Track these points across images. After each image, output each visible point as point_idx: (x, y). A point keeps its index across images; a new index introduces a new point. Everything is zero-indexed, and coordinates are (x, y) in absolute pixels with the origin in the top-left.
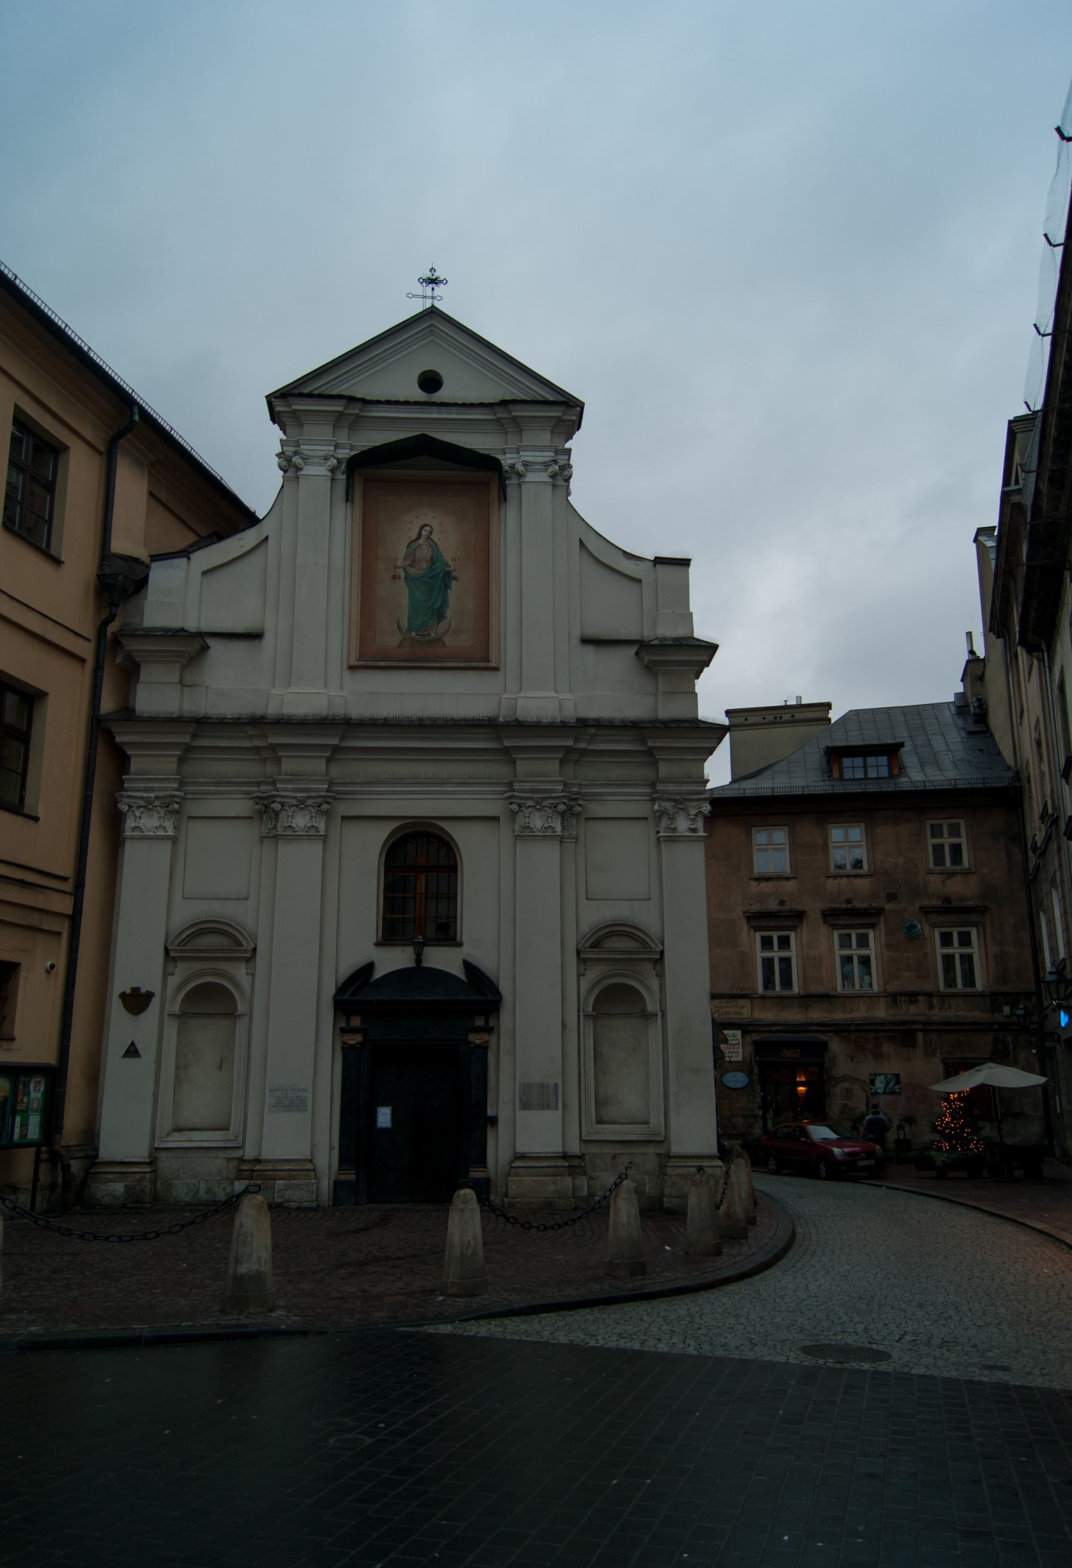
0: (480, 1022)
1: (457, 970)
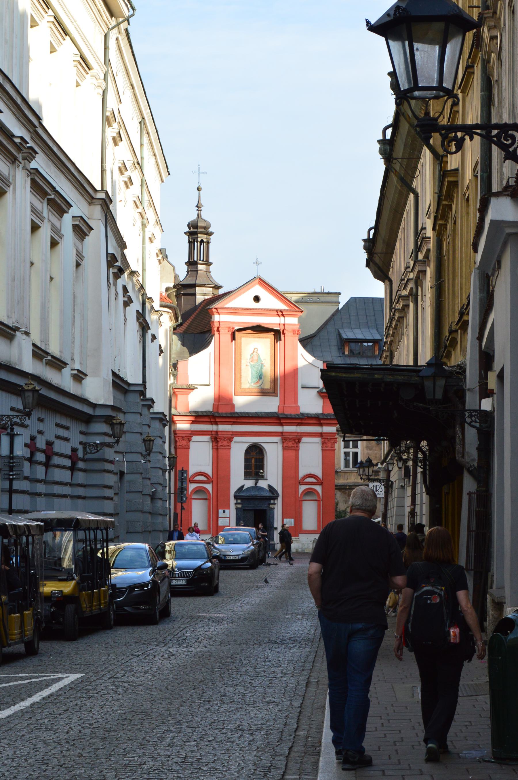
0: (272, 502)
1: (266, 487)
